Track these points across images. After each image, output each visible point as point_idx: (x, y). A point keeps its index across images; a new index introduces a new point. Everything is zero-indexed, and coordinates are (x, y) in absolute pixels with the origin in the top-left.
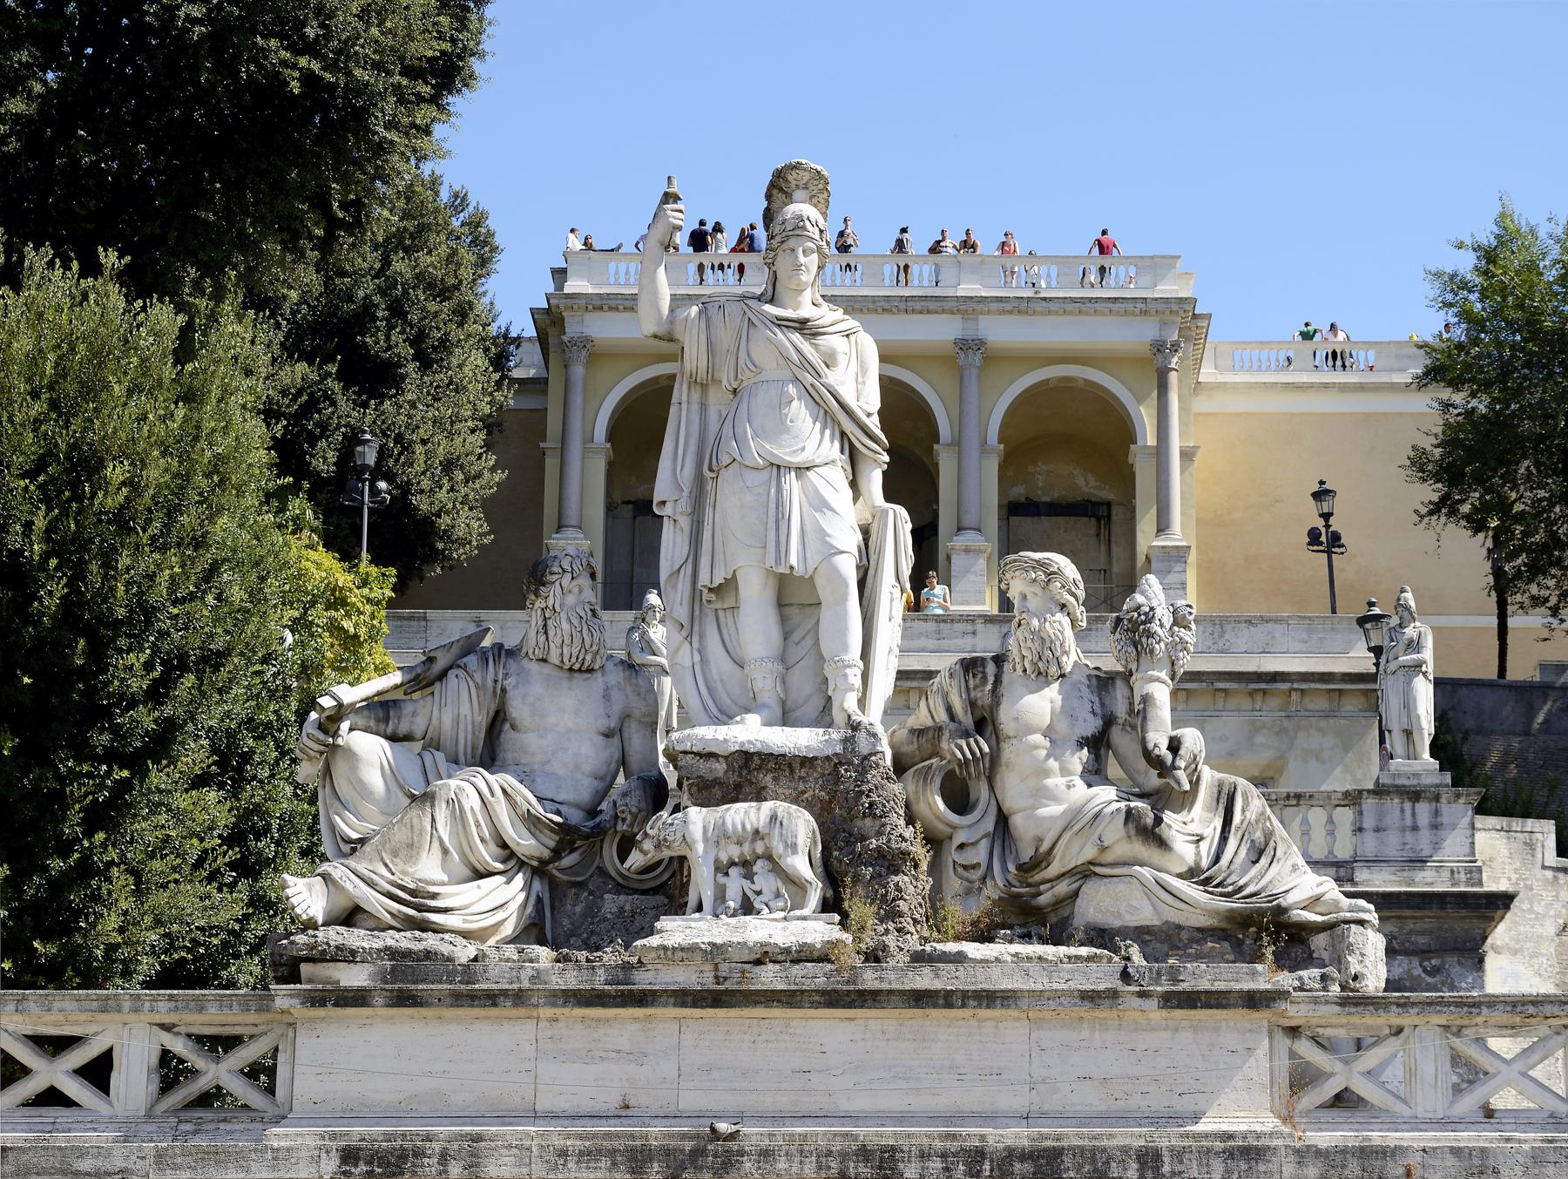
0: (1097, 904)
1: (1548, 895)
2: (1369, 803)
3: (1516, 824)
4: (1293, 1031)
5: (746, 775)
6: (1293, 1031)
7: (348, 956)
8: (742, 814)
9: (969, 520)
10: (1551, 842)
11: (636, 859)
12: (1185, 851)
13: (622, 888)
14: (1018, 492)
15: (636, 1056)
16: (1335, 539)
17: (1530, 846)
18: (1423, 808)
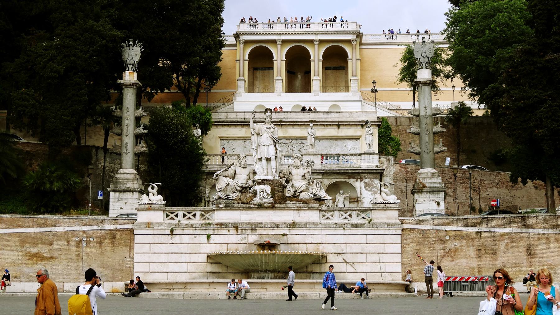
0: (303, 196)
1: (392, 167)
2: (363, 156)
3: (387, 157)
4: (322, 211)
5: (263, 182)
6: (322, 211)
7: (220, 204)
8: (262, 187)
9: (316, 74)
10: (393, 159)
11: (251, 191)
12: (311, 190)
13: (250, 193)
14: (328, 65)
15: (251, 214)
16: (376, 90)
17: (389, 160)
18: (371, 156)
